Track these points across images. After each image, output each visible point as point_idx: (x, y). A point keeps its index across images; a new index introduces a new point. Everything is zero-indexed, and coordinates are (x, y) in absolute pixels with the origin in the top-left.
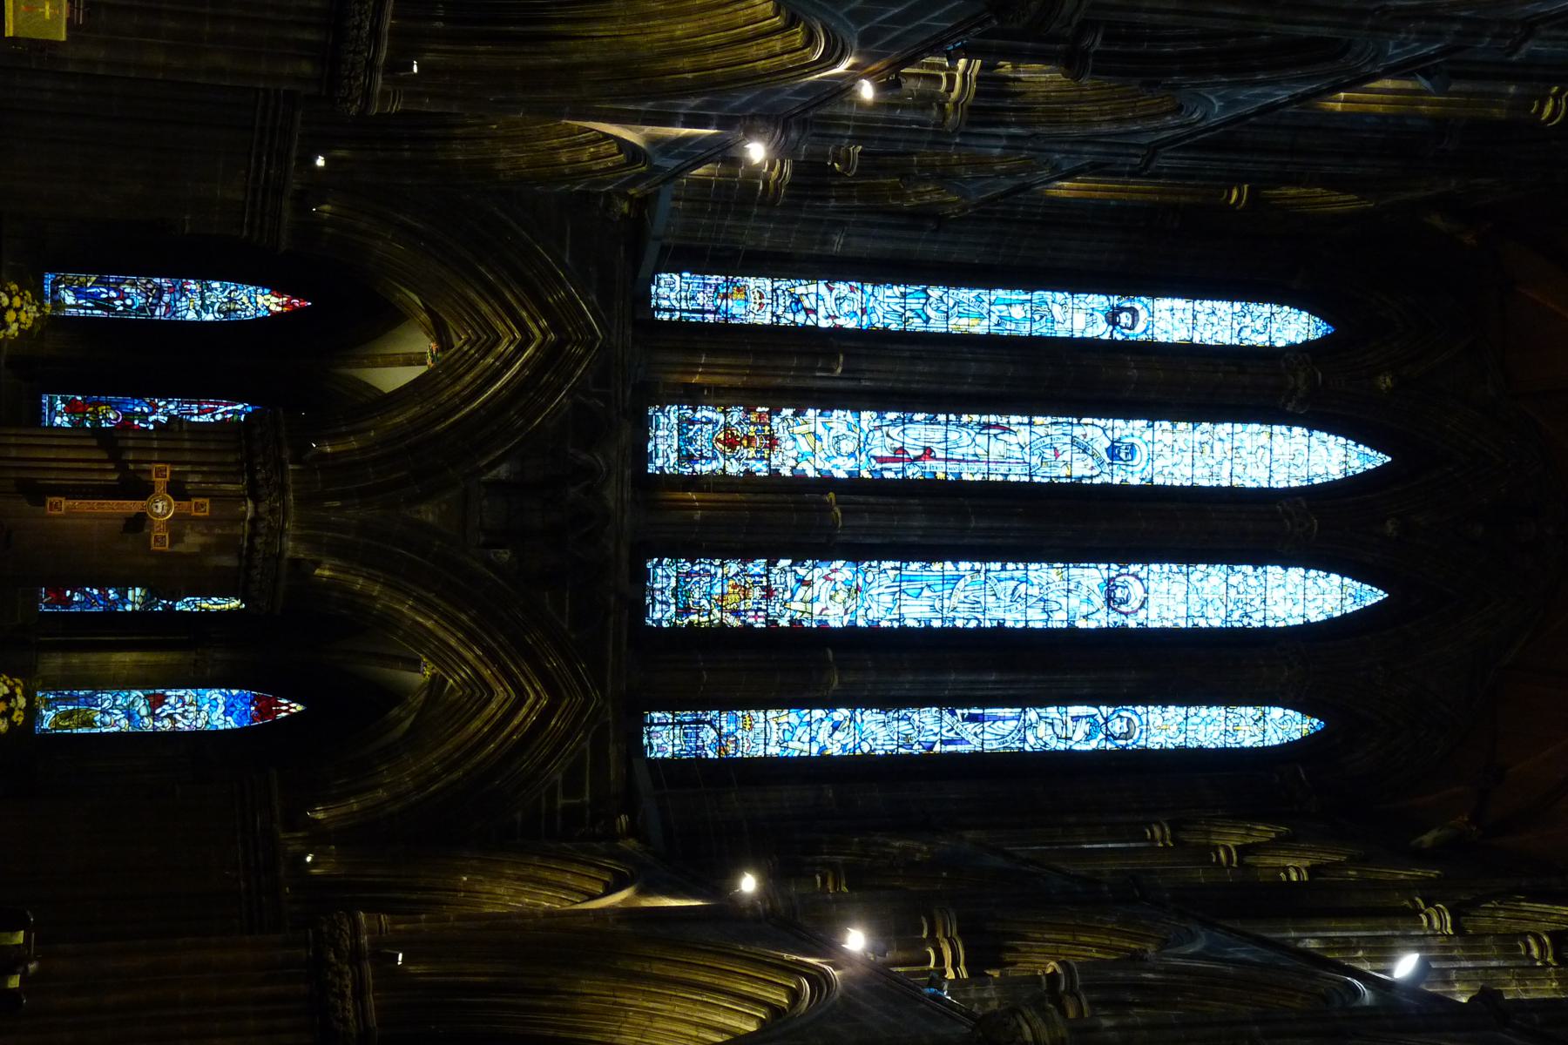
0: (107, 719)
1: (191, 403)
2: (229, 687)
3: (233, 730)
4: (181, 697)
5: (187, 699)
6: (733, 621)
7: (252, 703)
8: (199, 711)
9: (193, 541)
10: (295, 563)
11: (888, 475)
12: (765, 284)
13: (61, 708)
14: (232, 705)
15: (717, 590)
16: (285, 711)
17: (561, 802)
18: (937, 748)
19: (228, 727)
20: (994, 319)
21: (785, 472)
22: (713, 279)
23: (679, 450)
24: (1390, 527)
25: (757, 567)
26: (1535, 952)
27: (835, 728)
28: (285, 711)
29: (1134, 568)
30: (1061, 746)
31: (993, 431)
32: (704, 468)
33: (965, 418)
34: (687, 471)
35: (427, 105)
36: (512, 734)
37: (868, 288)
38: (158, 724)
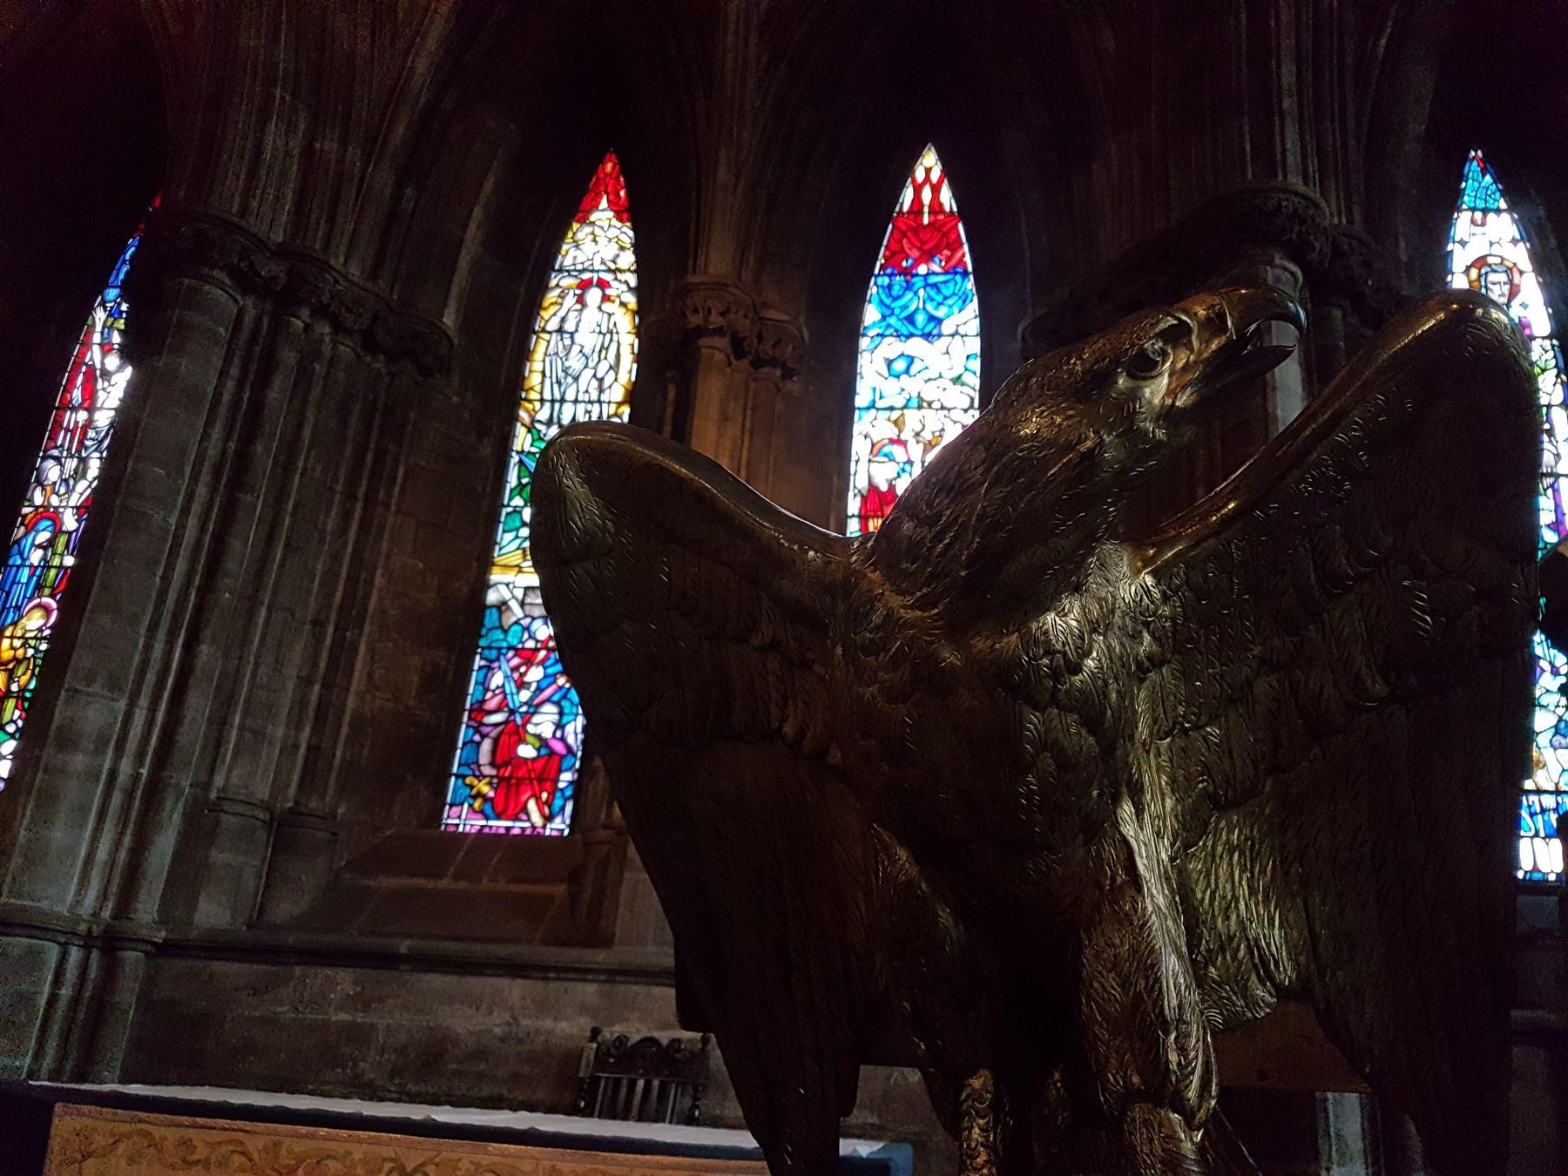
1: (58, 424)
2: (853, 331)
3: (985, 314)
4: (876, 450)
5: (884, 430)
7: (908, 273)
14: (910, 319)
16: (936, 189)
19: (974, 326)
28: (936, 189)
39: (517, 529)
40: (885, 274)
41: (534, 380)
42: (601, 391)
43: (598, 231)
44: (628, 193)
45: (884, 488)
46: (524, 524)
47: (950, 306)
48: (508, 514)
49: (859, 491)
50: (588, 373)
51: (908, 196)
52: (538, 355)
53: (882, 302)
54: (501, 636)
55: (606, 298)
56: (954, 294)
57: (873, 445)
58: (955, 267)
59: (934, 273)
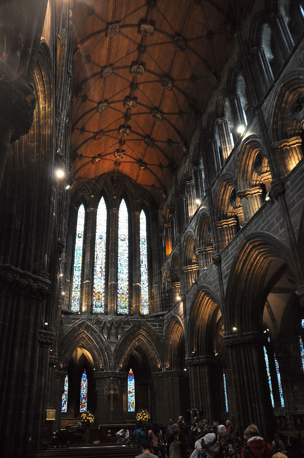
0: (133, 400)
2: (128, 381)
6: (127, 300)
9: (116, 387)
10: (120, 371)
11: (104, 274)
12: (73, 293)
13: (131, 407)
15: (123, 302)
17: (158, 327)
18: (147, 268)
20: (79, 256)
21: (104, 290)
22: (72, 301)
23: (100, 308)
24: (115, 197)
25: (119, 295)
26: (189, 183)
27: (144, 284)
29: (119, 236)
30: (146, 249)
31: (97, 257)
32: (103, 304)
33: (95, 261)
34: (104, 306)
35: (57, 349)
36: (147, 336)
37: (74, 276)
38: (133, 392)
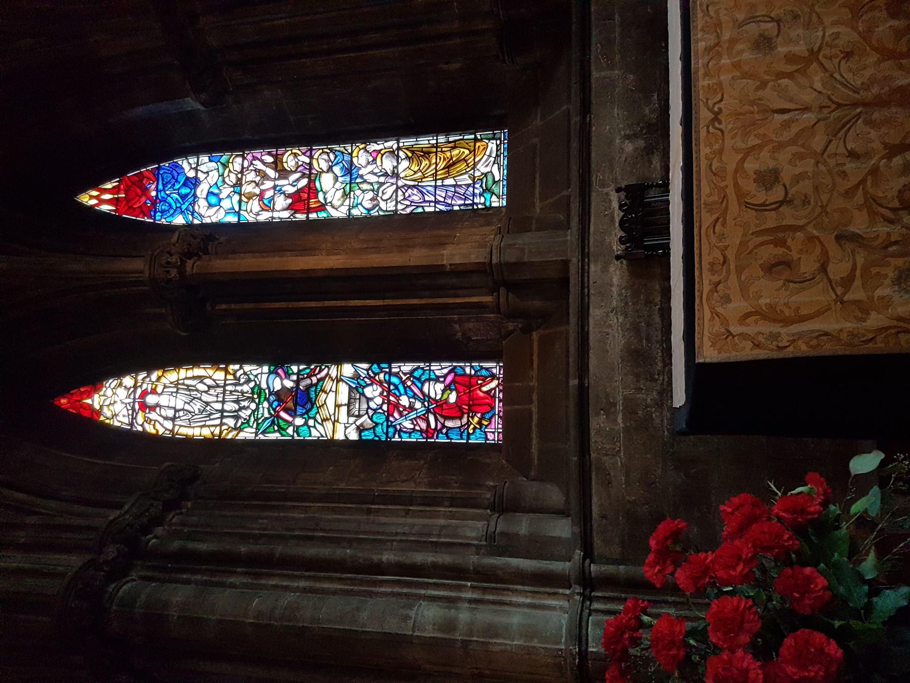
0: (388, 164)
4: (265, 208)
5: (255, 205)
7: (154, 202)
8: (239, 183)
14: (184, 197)
19: (193, 160)
39: (309, 427)
40: (155, 216)
41: (206, 432)
42: (218, 386)
43: (107, 403)
44: (83, 386)
45: (290, 201)
46: (306, 424)
47: (178, 174)
48: (298, 435)
49: (292, 215)
50: (205, 397)
51: (105, 208)
52: (189, 432)
53: (172, 215)
54: (380, 427)
55: (154, 391)
56: (170, 174)
57: (263, 210)
58: (154, 175)
59: (157, 187)
